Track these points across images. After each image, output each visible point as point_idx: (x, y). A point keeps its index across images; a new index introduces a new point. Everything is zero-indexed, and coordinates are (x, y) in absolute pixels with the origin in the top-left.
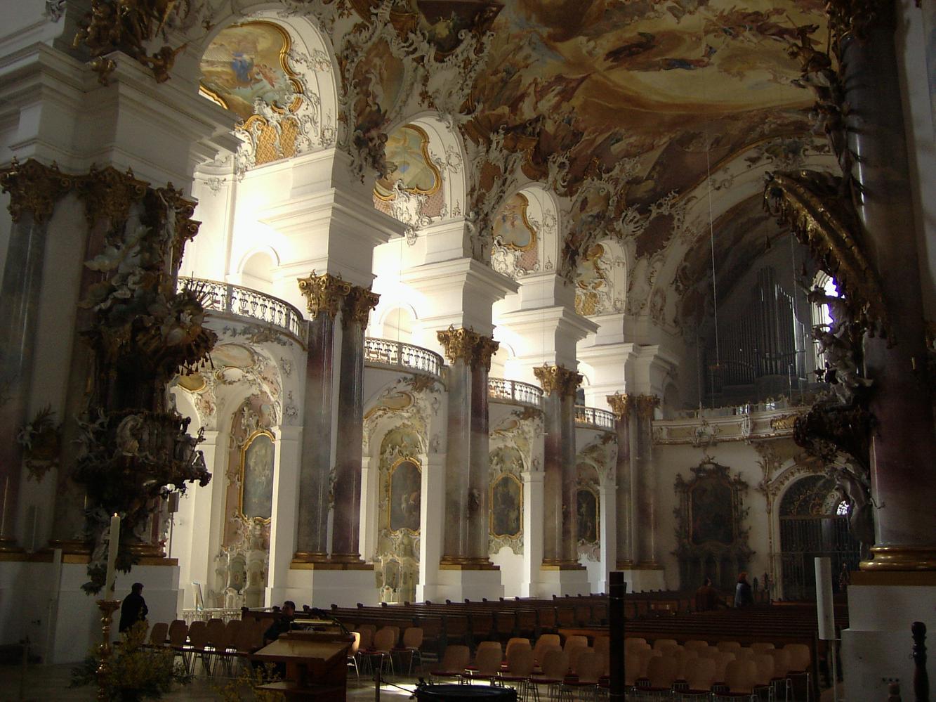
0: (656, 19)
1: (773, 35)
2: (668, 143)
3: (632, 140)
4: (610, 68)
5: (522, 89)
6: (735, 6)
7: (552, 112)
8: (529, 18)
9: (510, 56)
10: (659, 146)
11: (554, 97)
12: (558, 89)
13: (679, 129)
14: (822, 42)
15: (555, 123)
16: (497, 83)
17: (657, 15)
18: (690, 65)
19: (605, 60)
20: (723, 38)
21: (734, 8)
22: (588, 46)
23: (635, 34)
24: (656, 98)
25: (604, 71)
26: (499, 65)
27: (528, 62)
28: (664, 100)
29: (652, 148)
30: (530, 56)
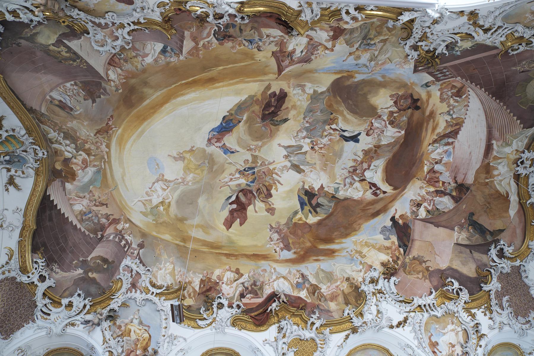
0: (296, 135)
1: (237, 197)
2: (102, 73)
3: (149, 60)
4: (268, 87)
5: (341, 39)
6: (282, 185)
7: (283, 40)
8: (383, 77)
9: (376, 53)
10: (108, 70)
11: (294, 49)
12: (298, 54)
13: (120, 91)
14: (230, 230)
15: (268, 36)
16: (375, 36)
17: (299, 137)
18: (217, 132)
19: (281, 90)
20: (243, 165)
21: (279, 182)
22: (310, 88)
23: (290, 116)
24: (192, 95)
25: (269, 85)
26: (384, 45)
27: (353, 56)
28: (180, 99)
29: (112, 62)
30: (355, 60)
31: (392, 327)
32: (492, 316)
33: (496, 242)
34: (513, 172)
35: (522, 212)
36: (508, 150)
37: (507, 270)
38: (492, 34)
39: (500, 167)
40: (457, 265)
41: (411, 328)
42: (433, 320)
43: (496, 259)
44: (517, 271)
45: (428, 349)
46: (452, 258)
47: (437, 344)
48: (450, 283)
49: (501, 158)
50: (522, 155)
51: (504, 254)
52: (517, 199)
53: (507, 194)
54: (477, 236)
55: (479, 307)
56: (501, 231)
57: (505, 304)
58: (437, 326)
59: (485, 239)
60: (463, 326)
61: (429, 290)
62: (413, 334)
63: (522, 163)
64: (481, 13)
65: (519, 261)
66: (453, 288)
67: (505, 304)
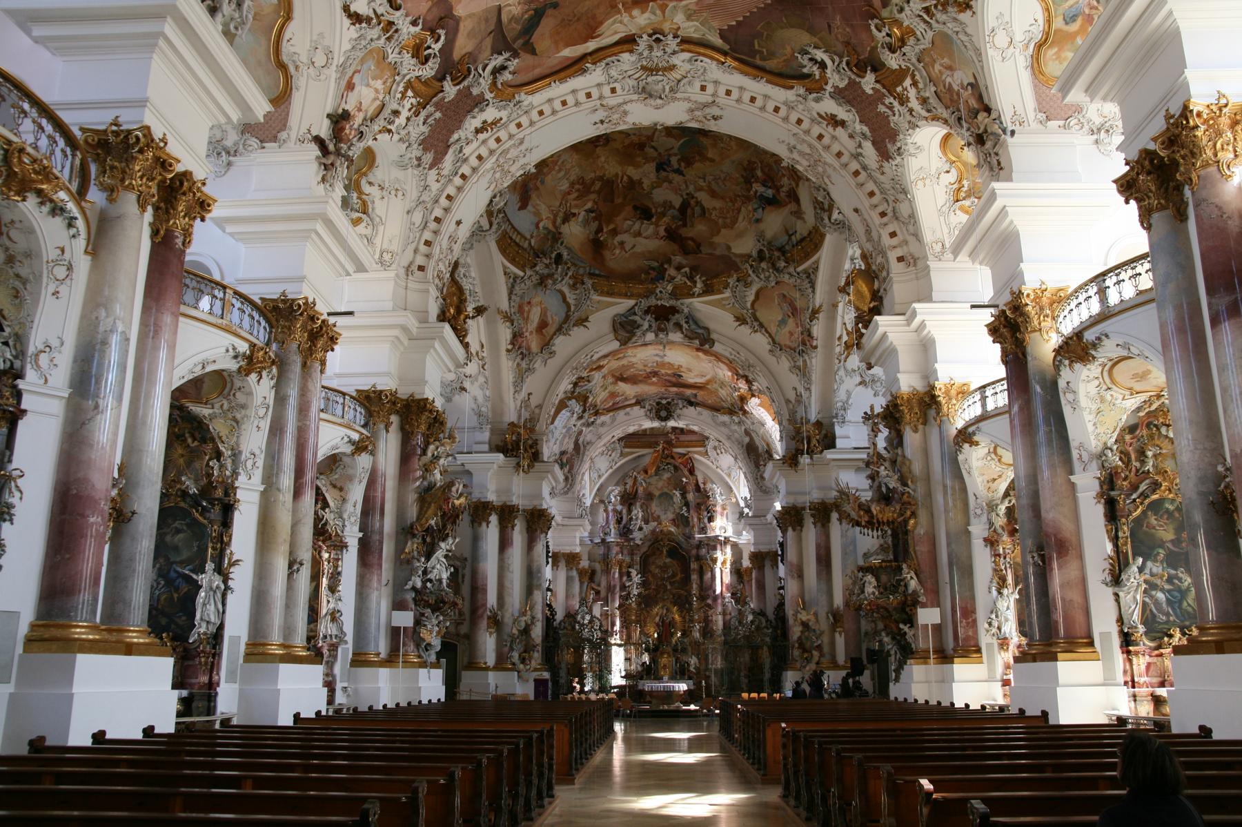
31: (346, 9)
32: (413, 118)
33: (515, 55)
34: (639, 32)
35: (569, 62)
36: (679, 18)
37: (475, 91)
38: (920, 16)
39: (647, 15)
40: (465, 27)
41: (355, 35)
42: (378, 55)
43: (489, 68)
44: (479, 102)
45: (344, 83)
46: (474, 14)
47: (353, 88)
48: (436, 36)
49: (663, 12)
50: (670, 37)
51: (500, 73)
52: (590, 50)
53: (599, 36)
54: (519, 27)
55: (416, 95)
56: (533, 52)
57: (431, 121)
58: (373, 68)
59: (515, 40)
60: (387, 98)
61: (417, 16)
62: (349, 47)
63: (658, 41)
64: (965, 17)
65: (492, 95)
66: (433, 46)
67: (431, 121)
